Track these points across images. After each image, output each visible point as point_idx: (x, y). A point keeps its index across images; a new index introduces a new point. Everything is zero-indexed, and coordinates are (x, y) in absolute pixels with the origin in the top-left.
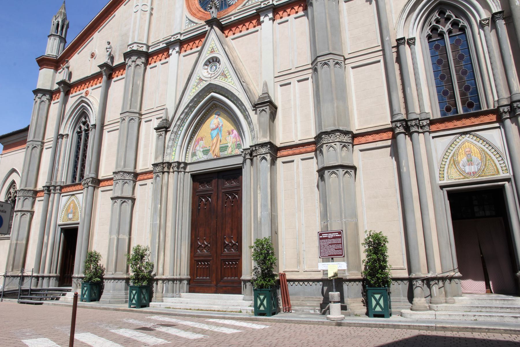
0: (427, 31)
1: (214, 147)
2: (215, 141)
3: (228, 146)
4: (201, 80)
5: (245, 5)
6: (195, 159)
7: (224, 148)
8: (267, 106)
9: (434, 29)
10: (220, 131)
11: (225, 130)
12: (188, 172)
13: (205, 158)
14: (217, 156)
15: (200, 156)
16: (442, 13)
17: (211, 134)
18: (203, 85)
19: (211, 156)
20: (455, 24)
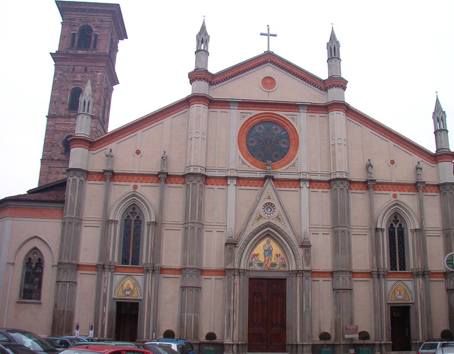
0: (389, 226)
1: (266, 263)
2: (267, 258)
3: (276, 264)
4: (260, 217)
5: (288, 168)
6: (251, 268)
7: (274, 265)
8: (306, 246)
9: (392, 225)
10: (271, 253)
11: (274, 253)
12: (247, 276)
13: (260, 268)
14: (269, 269)
15: (256, 267)
16: (396, 217)
17: (264, 253)
18: (262, 222)
19: (263, 268)
20: (400, 225)
